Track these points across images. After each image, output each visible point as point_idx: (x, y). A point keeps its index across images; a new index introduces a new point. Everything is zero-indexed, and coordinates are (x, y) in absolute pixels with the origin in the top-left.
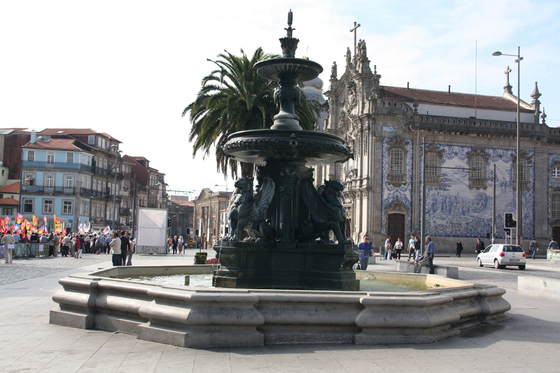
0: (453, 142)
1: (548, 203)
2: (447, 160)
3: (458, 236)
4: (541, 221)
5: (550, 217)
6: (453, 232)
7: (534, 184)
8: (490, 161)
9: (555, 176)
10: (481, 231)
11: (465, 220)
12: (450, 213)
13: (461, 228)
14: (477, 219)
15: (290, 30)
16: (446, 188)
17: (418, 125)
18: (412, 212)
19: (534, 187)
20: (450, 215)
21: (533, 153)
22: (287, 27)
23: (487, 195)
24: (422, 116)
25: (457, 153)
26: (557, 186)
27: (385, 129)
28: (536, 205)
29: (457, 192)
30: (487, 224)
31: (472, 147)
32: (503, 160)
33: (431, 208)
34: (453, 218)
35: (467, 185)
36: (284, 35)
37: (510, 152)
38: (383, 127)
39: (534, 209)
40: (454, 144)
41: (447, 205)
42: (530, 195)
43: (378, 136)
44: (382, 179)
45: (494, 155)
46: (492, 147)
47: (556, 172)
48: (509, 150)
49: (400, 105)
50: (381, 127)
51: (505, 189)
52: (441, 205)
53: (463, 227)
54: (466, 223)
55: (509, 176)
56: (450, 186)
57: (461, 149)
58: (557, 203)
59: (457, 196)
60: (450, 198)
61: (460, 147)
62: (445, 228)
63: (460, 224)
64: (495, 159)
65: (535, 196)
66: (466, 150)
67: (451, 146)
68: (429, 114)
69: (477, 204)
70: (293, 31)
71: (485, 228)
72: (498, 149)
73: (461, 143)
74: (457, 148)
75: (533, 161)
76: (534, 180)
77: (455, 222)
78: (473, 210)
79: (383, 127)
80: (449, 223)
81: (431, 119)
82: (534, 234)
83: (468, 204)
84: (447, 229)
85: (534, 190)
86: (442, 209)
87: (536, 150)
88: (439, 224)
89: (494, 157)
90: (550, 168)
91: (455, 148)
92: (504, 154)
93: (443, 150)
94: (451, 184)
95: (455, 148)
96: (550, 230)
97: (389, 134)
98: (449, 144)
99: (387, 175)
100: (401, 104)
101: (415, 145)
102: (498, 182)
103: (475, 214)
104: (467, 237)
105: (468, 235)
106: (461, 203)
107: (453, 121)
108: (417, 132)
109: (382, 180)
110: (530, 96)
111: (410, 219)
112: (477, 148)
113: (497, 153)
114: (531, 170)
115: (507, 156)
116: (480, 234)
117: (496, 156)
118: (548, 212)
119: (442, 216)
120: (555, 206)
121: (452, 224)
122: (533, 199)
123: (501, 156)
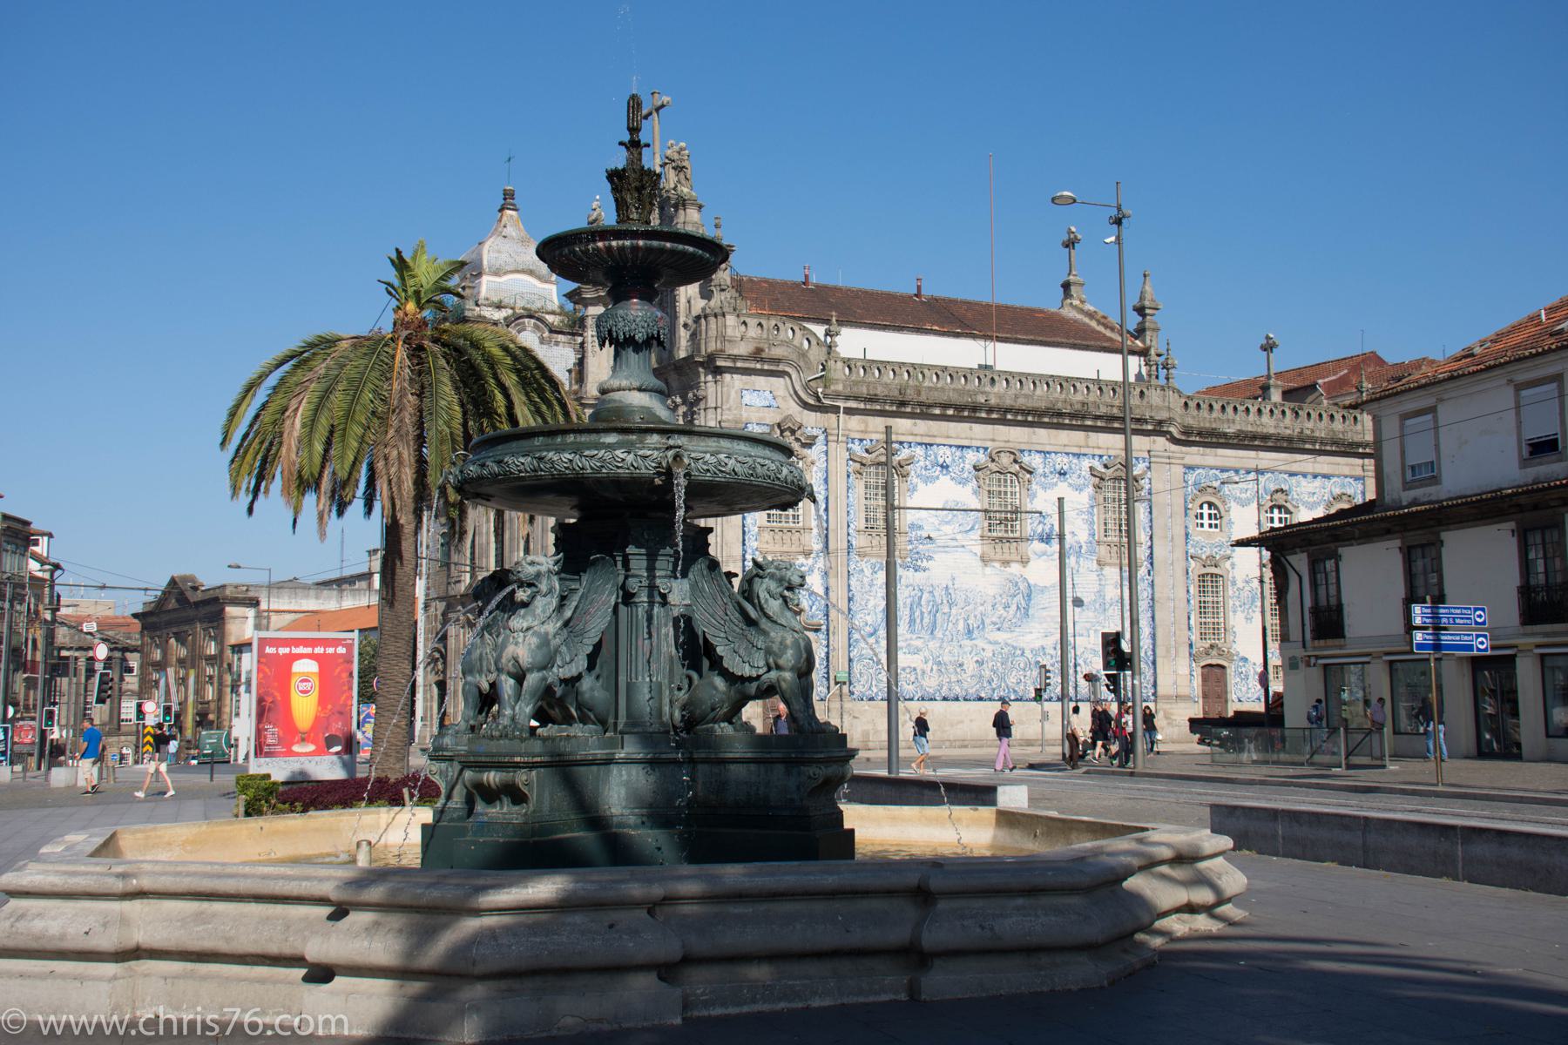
0: (935, 436)
1: (1188, 601)
2: (921, 486)
3: (957, 699)
4: (1173, 652)
5: (1193, 638)
6: (941, 686)
7: (1151, 547)
8: (1034, 486)
9: (1202, 525)
10: (1018, 683)
11: (974, 653)
12: (932, 633)
13: (964, 676)
14: (1006, 650)
15: (634, 145)
16: (919, 563)
17: (840, 387)
18: (828, 634)
19: (1151, 556)
20: (934, 638)
21: (1147, 464)
22: (626, 138)
23: (1031, 582)
24: (849, 363)
25: (947, 467)
26: (1208, 554)
27: (748, 398)
28: (1157, 606)
29: (949, 577)
30: (1033, 661)
31: (986, 449)
32: (1070, 485)
33: (879, 620)
34: (940, 647)
35: (976, 554)
36: (619, 160)
37: (1086, 463)
38: (744, 392)
39: (1153, 618)
40: (938, 441)
41: (924, 610)
43: (730, 418)
44: (744, 540)
45: (1046, 470)
46: (1039, 448)
47: (1206, 516)
48: (1085, 455)
49: (790, 332)
50: (736, 392)
51: (1077, 562)
52: (907, 612)
53: (969, 673)
54: (977, 662)
55: (1086, 527)
56: (930, 558)
57: (958, 453)
58: (1210, 599)
59: (950, 585)
60: (930, 592)
61: (954, 449)
62: (919, 677)
63: (961, 665)
64: (1049, 480)
65: (1155, 582)
66: (972, 457)
67: (931, 445)
68: (867, 358)
69: (1005, 608)
70: (645, 150)
71: (1028, 673)
72: (1056, 453)
73: (957, 438)
74: (947, 451)
75: (1147, 487)
76: (1151, 538)
77: (946, 658)
78: (995, 624)
79: (744, 392)
80: (930, 663)
81: (877, 372)
82: (1155, 685)
83: (981, 608)
84: (927, 679)
85: (1152, 564)
86: (912, 622)
87: (1155, 456)
88: (905, 665)
89: (1045, 476)
90: (1190, 506)
91: (941, 452)
93: (910, 461)
94: (934, 552)
95: (941, 452)
96: (1194, 673)
97: (761, 415)
98: (927, 440)
99: (756, 529)
100: (792, 329)
101: (832, 445)
103: (1001, 637)
104: (980, 699)
105: (983, 695)
106: (962, 605)
107: (934, 376)
108: (839, 407)
109: (744, 544)
111: (823, 655)
112: (999, 452)
114: (1142, 510)
116: (1015, 691)
117: (1051, 473)
118: (1189, 624)
119: (912, 642)
120: (1205, 607)
121: (939, 663)
122: (1149, 590)
123: (1065, 474)
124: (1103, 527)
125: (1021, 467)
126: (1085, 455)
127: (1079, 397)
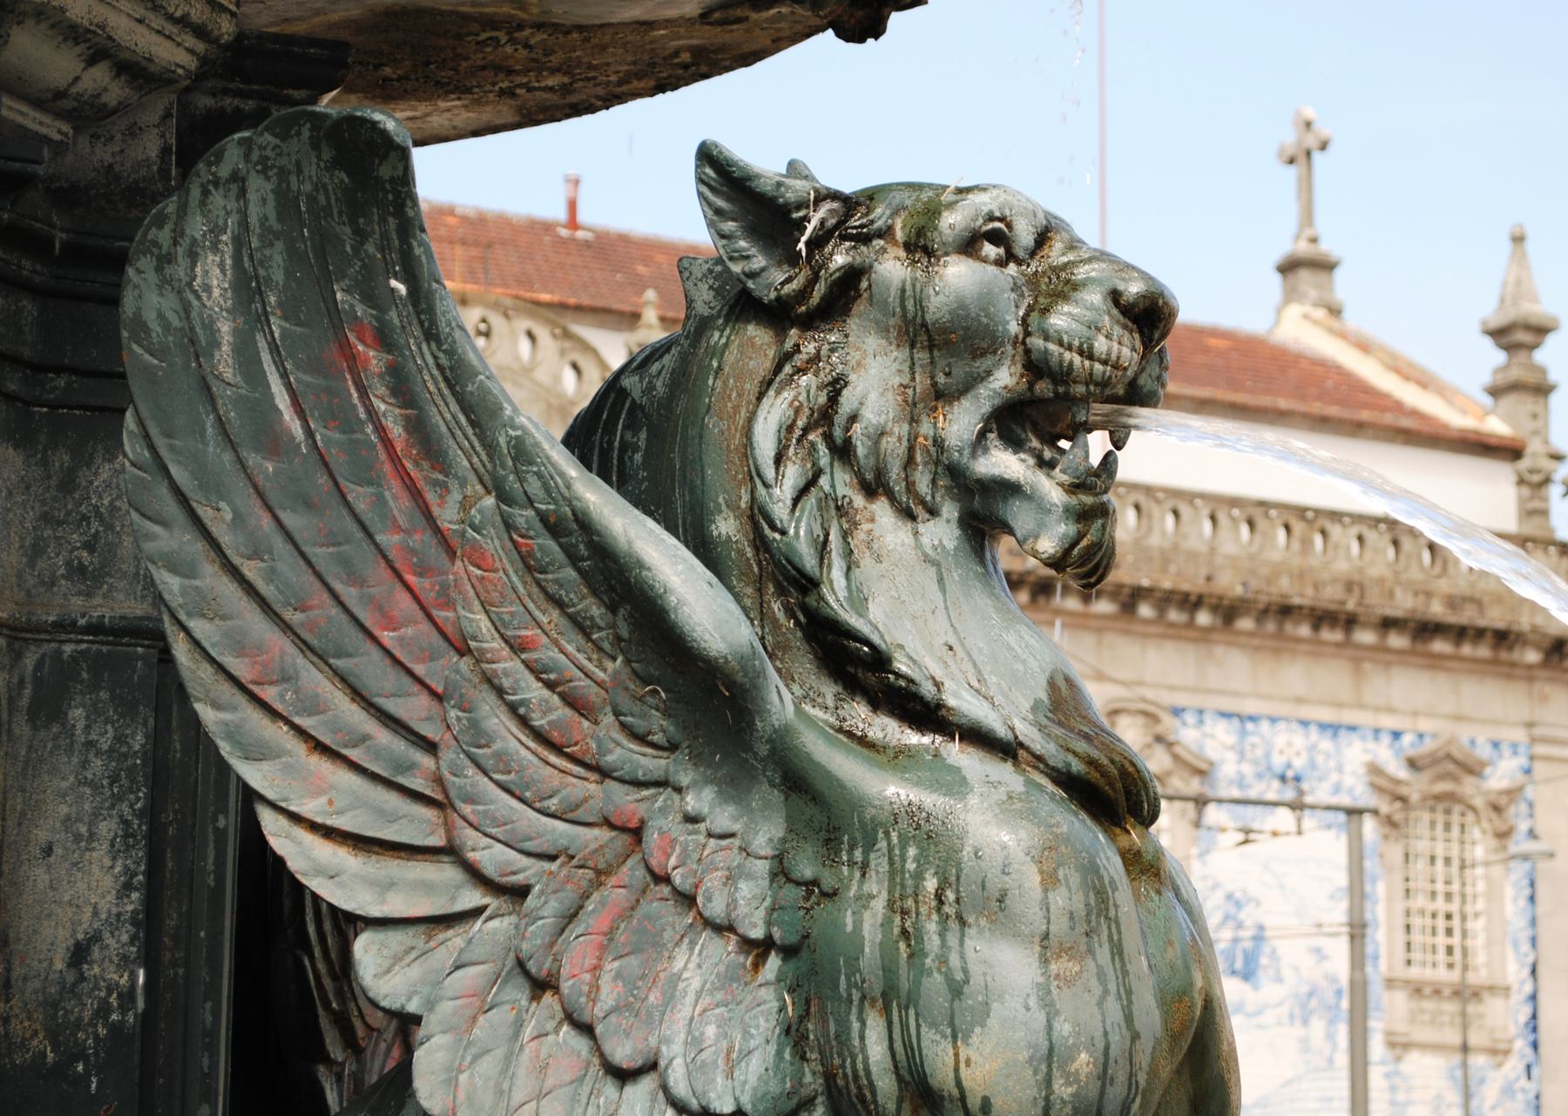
42: (1508, 1091)
46: (1227, 704)
48: (1352, 728)
65: (1545, 1100)
72: (1273, 720)
76: (1534, 971)
85: (1535, 1046)
92: (1313, 765)
102: (1279, 979)
110: (1475, 328)
113: (1268, 755)
114: (1509, 892)
115: (1334, 777)
124: (1400, 938)
125: (1176, 758)
126: (1352, 728)
127: (1342, 566)
